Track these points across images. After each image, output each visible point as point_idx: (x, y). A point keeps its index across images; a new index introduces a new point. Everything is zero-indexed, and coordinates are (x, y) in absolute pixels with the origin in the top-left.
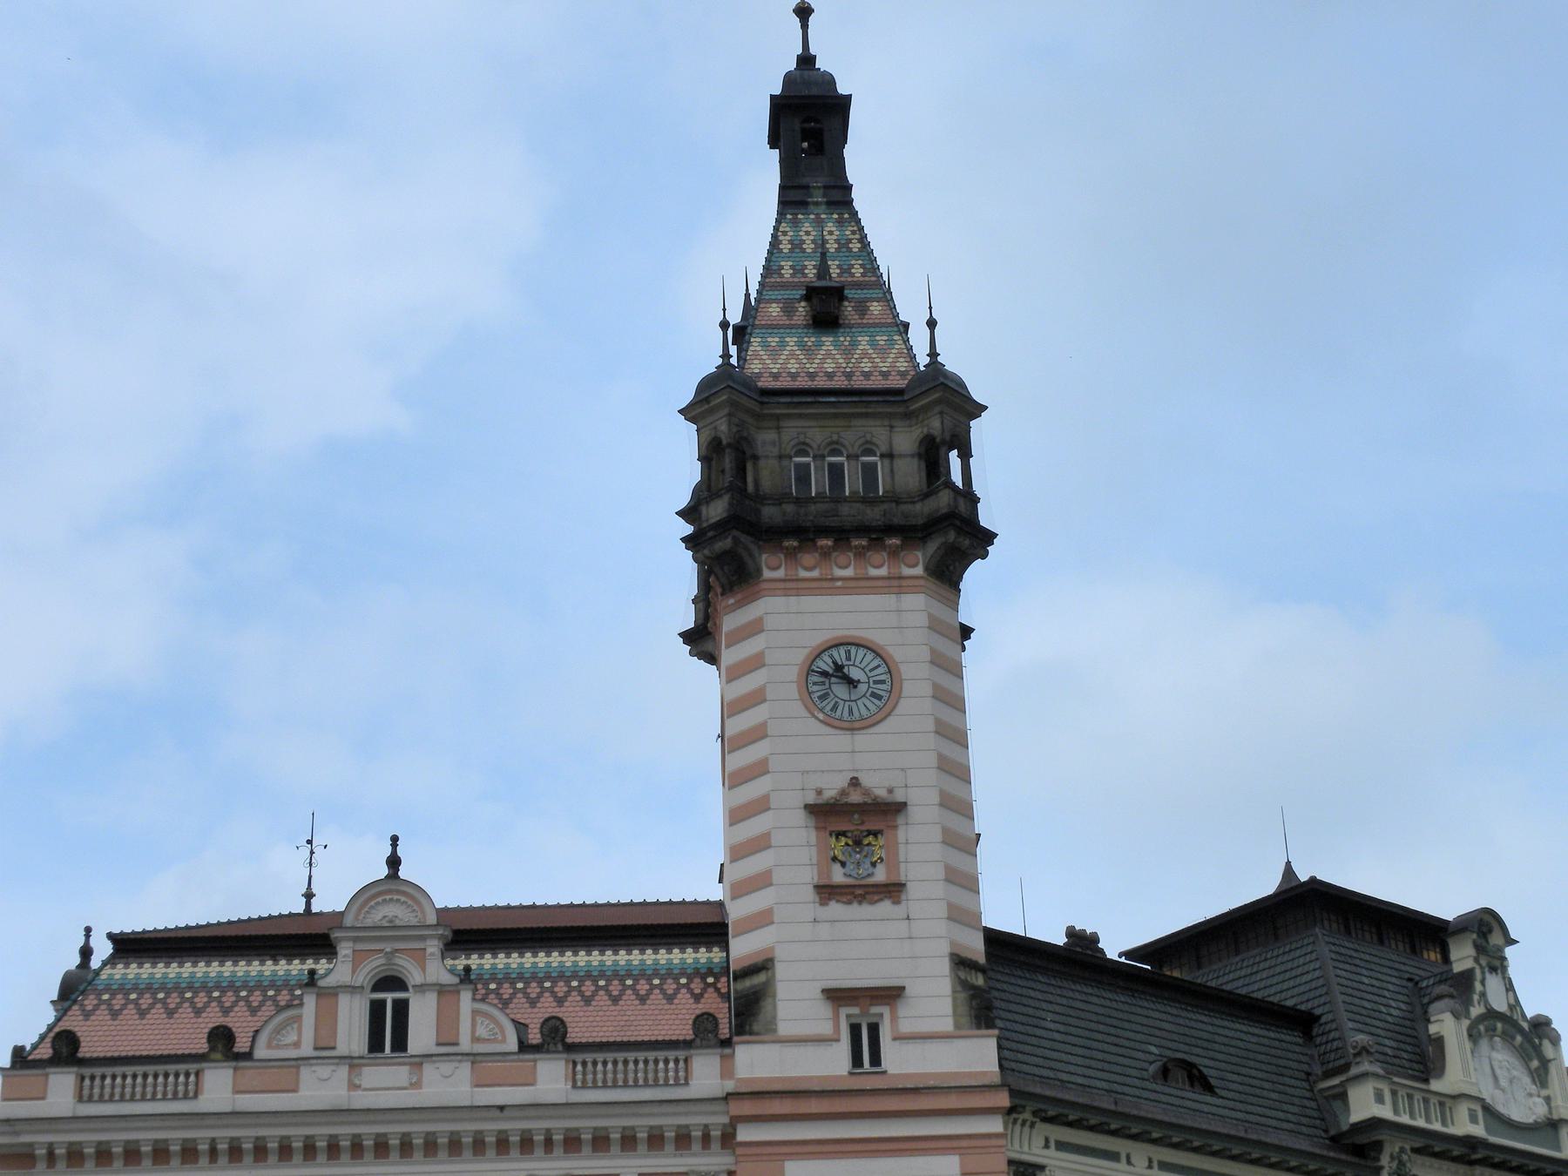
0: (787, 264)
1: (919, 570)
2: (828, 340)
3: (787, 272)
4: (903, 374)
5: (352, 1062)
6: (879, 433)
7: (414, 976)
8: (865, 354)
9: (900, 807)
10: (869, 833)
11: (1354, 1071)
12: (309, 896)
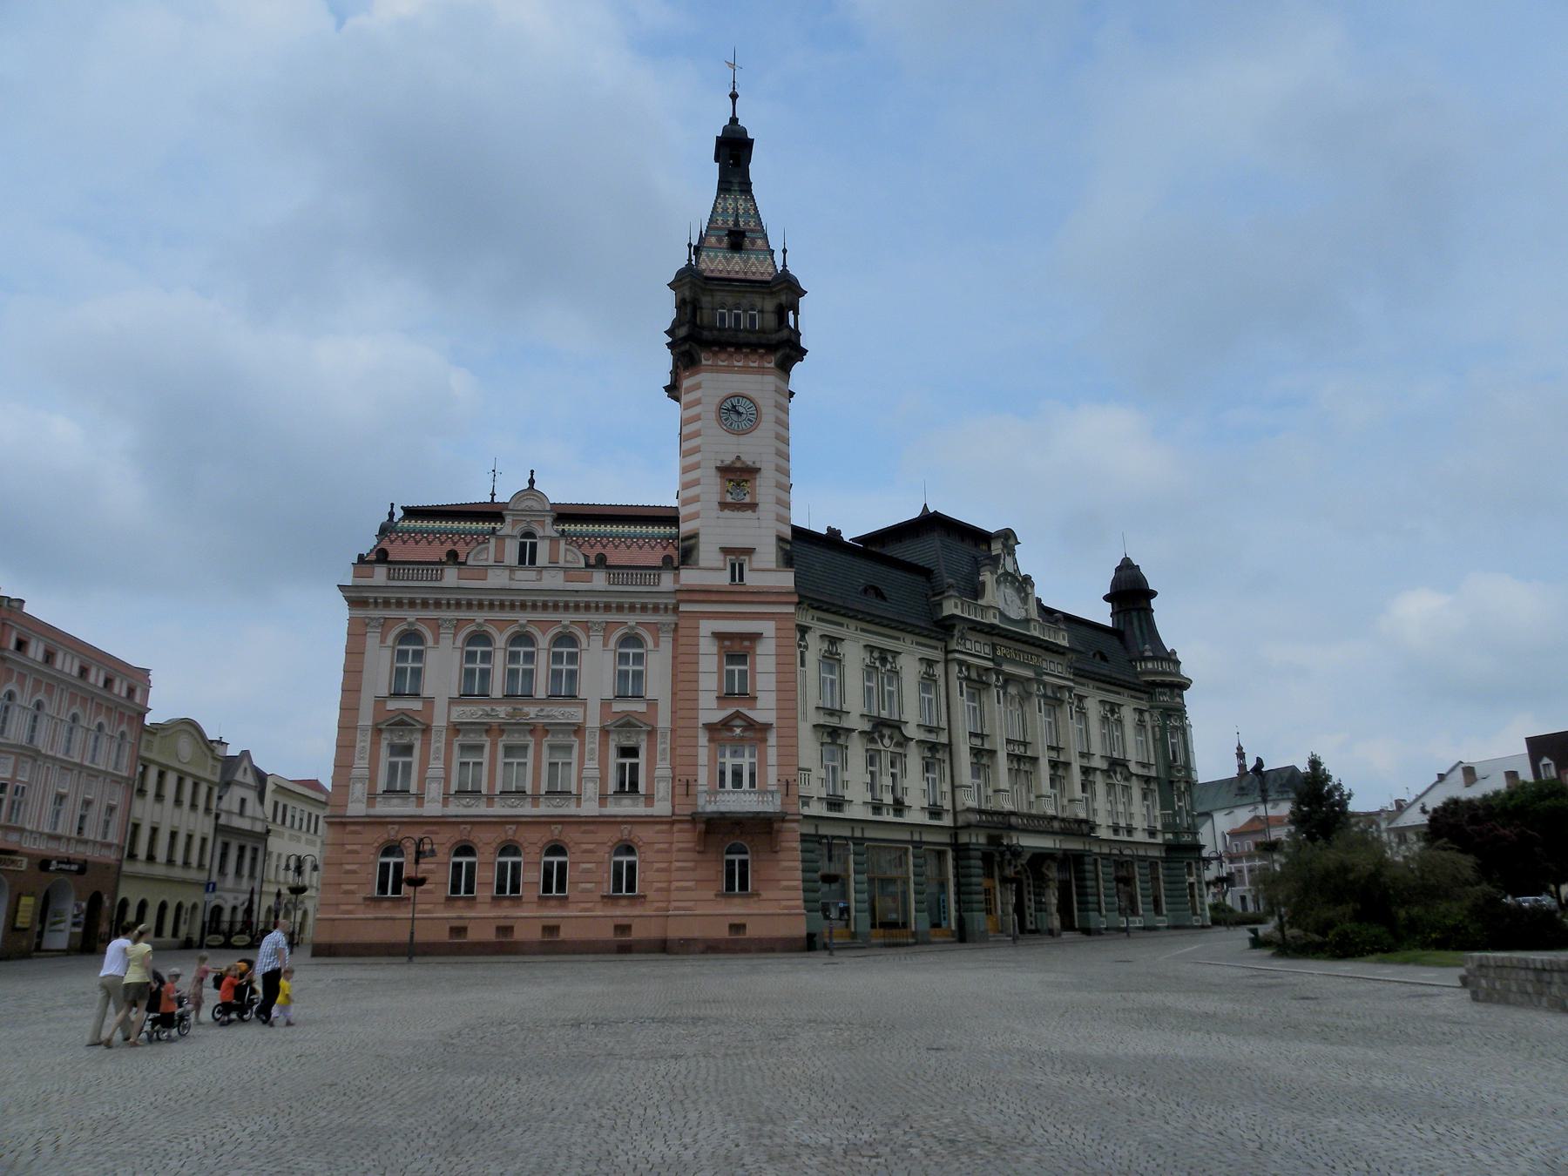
0: (720, 218)
1: (772, 365)
2: (737, 255)
3: (720, 222)
4: (770, 274)
5: (511, 568)
6: (758, 301)
7: (539, 532)
8: (753, 264)
9: (758, 470)
10: (744, 481)
11: (946, 594)
12: (493, 495)
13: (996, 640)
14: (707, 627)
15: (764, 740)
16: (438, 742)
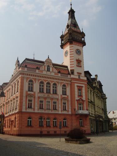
7: (50, 66)
13: (98, 91)
14: (76, 85)
15: (84, 103)
16: (36, 100)
